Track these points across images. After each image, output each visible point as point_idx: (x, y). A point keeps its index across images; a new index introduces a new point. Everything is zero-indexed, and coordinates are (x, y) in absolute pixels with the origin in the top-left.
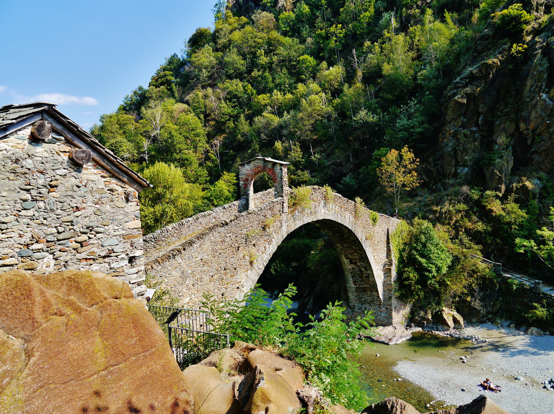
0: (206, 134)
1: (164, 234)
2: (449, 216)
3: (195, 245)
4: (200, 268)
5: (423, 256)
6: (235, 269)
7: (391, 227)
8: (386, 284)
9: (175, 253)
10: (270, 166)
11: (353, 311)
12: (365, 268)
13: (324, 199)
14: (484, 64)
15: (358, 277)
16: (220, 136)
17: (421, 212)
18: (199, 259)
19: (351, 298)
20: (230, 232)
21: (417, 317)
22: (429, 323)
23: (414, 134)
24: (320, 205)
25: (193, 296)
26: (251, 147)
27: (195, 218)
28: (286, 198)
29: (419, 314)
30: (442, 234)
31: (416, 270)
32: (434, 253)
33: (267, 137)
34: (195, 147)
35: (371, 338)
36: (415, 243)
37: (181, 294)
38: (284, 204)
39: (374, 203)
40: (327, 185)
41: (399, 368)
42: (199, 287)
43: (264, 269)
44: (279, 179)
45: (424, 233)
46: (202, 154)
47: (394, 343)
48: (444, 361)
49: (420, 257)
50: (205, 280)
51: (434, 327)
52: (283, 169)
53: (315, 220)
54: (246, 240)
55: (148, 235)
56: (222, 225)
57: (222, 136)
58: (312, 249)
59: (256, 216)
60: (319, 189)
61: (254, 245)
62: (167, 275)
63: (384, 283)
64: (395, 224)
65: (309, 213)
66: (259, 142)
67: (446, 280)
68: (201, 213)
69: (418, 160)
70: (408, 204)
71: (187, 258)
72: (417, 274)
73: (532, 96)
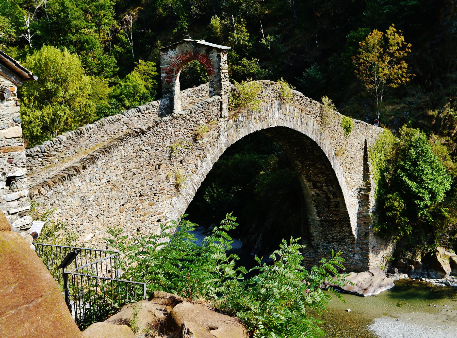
0: (114, 6)
1: (55, 147)
2: (449, 123)
3: (99, 162)
4: (106, 194)
5: (412, 178)
6: (155, 195)
7: (370, 139)
8: (360, 215)
9: (71, 173)
10: (203, 52)
11: (316, 252)
12: (334, 194)
13: (278, 98)
15: (323, 206)
16: (133, 9)
17: (411, 118)
18: (105, 181)
19: (314, 234)
20: (148, 144)
21: (402, 260)
22: (418, 268)
23: (406, 9)
24: (273, 106)
25: (97, 231)
26: (177, 26)
27: (99, 124)
28: (225, 97)
29: (404, 256)
30: (439, 148)
31: (402, 197)
32: (427, 174)
33: (199, 11)
34: (98, 25)
35: (340, 288)
36: (402, 160)
37: (80, 229)
38: (223, 105)
39: (348, 105)
40: (282, 79)
41: (377, 327)
42: (105, 219)
43: (194, 195)
44: (216, 71)
45: (415, 147)
46: (108, 34)
47: (370, 294)
48: (437, 318)
49: (408, 179)
50: (114, 209)
51: (424, 273)
52: (222, 55)
53: (265, 127)
54: (170, 154)
55: (34, 148)
56: (136, 134)
57: (136, 10)
58: (261, 168)
59: (183, 122)
60: (272, 84)
61: (181, 162)
62: (61, 203)
63: (359, 214)
64: (375, 135)
65: (257, 118)
66: (188, 17)
67: (443, 210)
68: (107, 118)
69: (410, 45)
70: (394, 107)
71: (87, 179)
72: (404, 203)
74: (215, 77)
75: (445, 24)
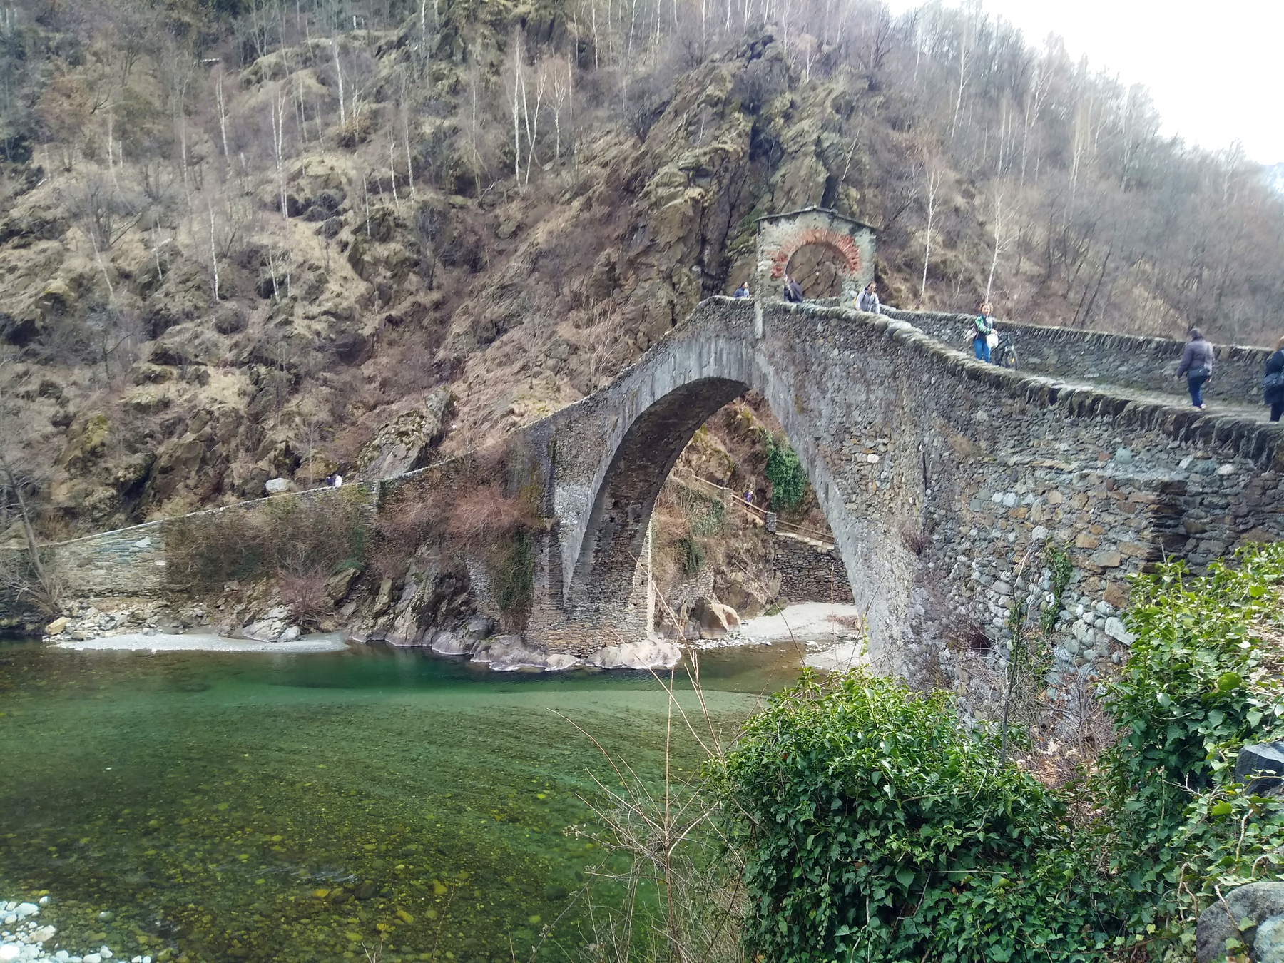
14: (716, 150)
75: (640, 292)
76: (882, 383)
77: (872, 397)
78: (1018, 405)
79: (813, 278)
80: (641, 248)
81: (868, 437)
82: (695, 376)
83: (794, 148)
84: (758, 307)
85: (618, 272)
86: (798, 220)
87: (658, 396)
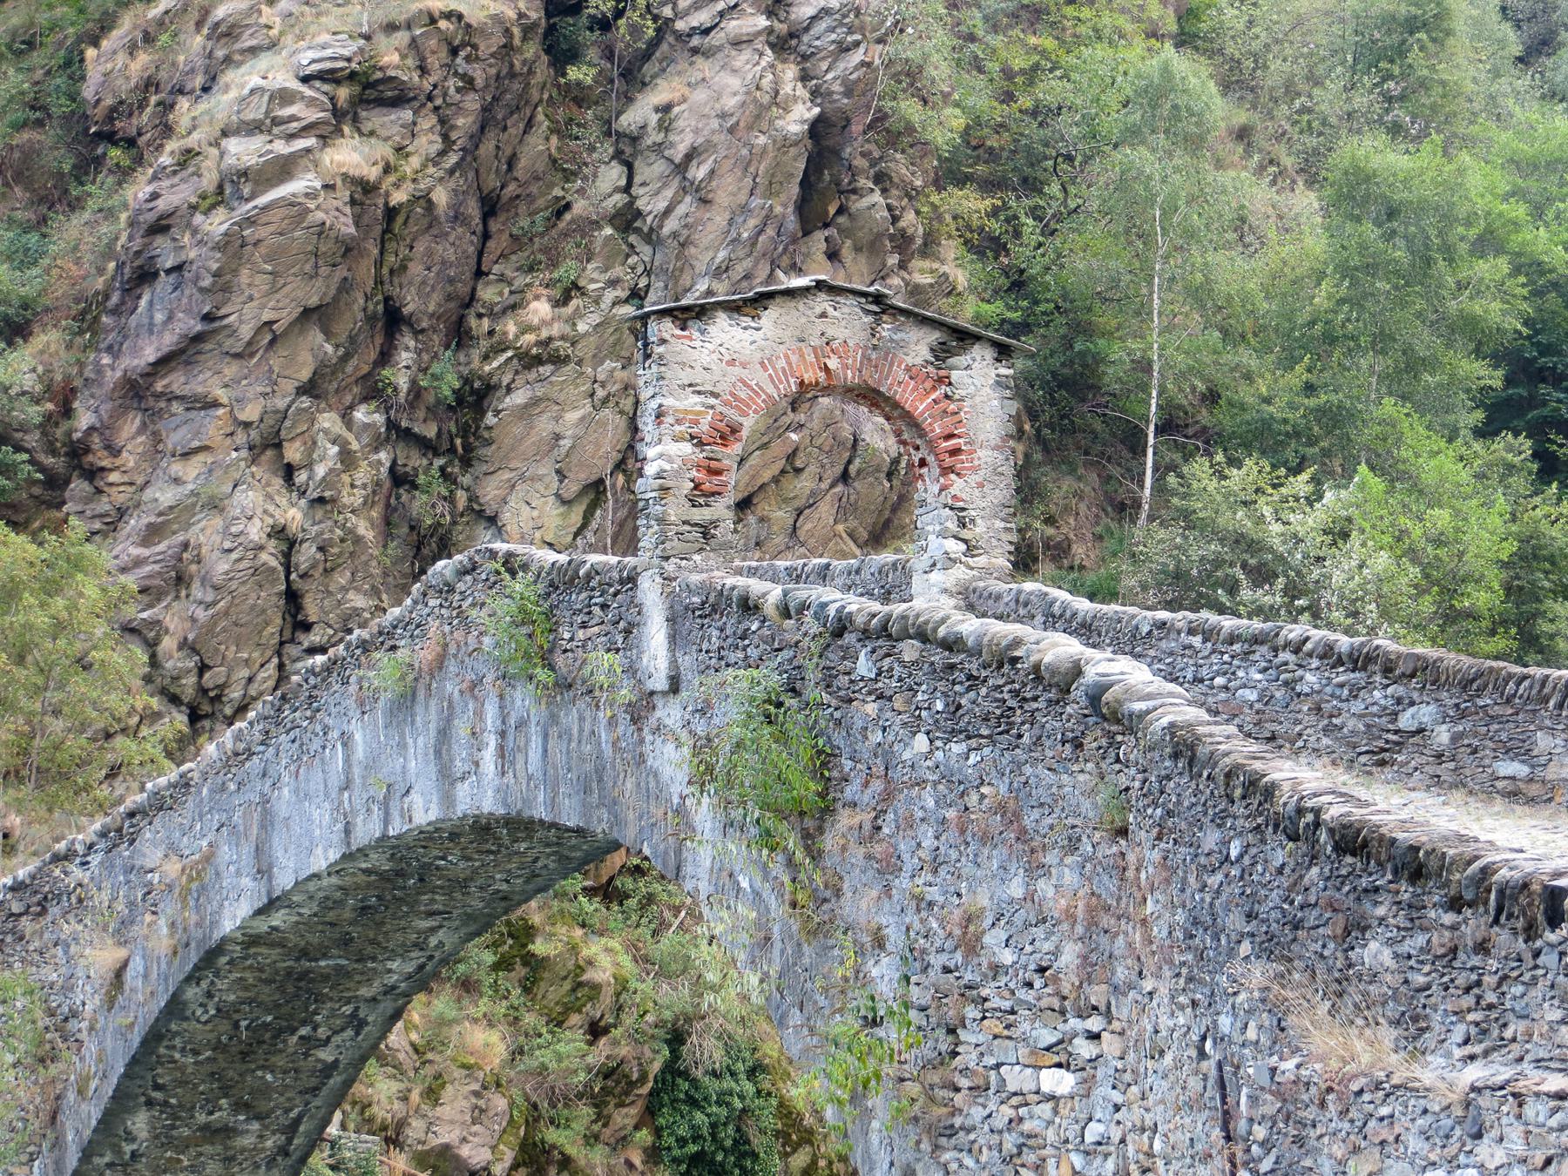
73: (739, 270)
74: (981, 485)
75: (165, 495)
76: (1073, 845)
77: (1045, 887)
78: (1473, 925)
79: (779, 449)
80: (169, 341)
81: (1038, 1012)
82: (424, 810)
83: (702, 18)
84: (650, 592)
85: (84, 419)
86: (770, 317)
87: (284, 880)
